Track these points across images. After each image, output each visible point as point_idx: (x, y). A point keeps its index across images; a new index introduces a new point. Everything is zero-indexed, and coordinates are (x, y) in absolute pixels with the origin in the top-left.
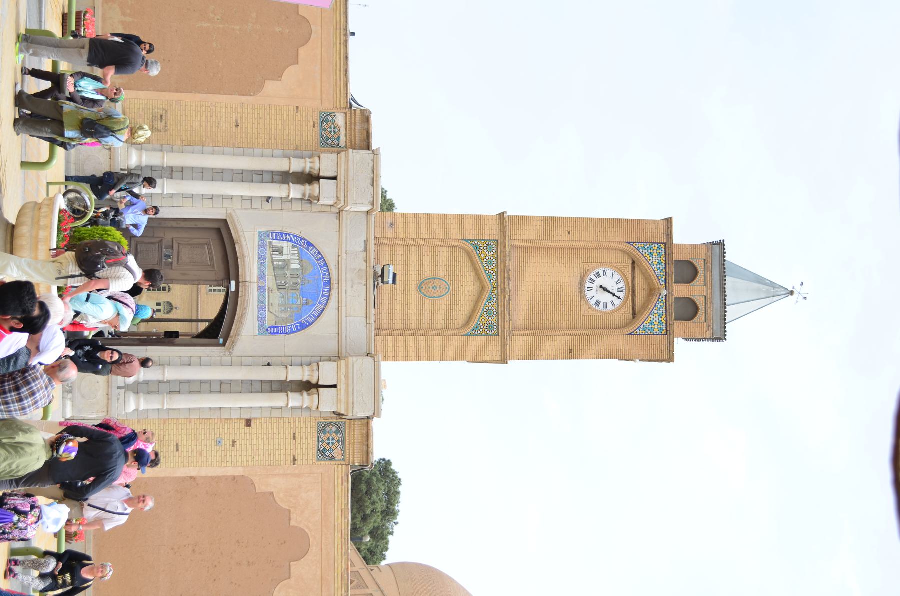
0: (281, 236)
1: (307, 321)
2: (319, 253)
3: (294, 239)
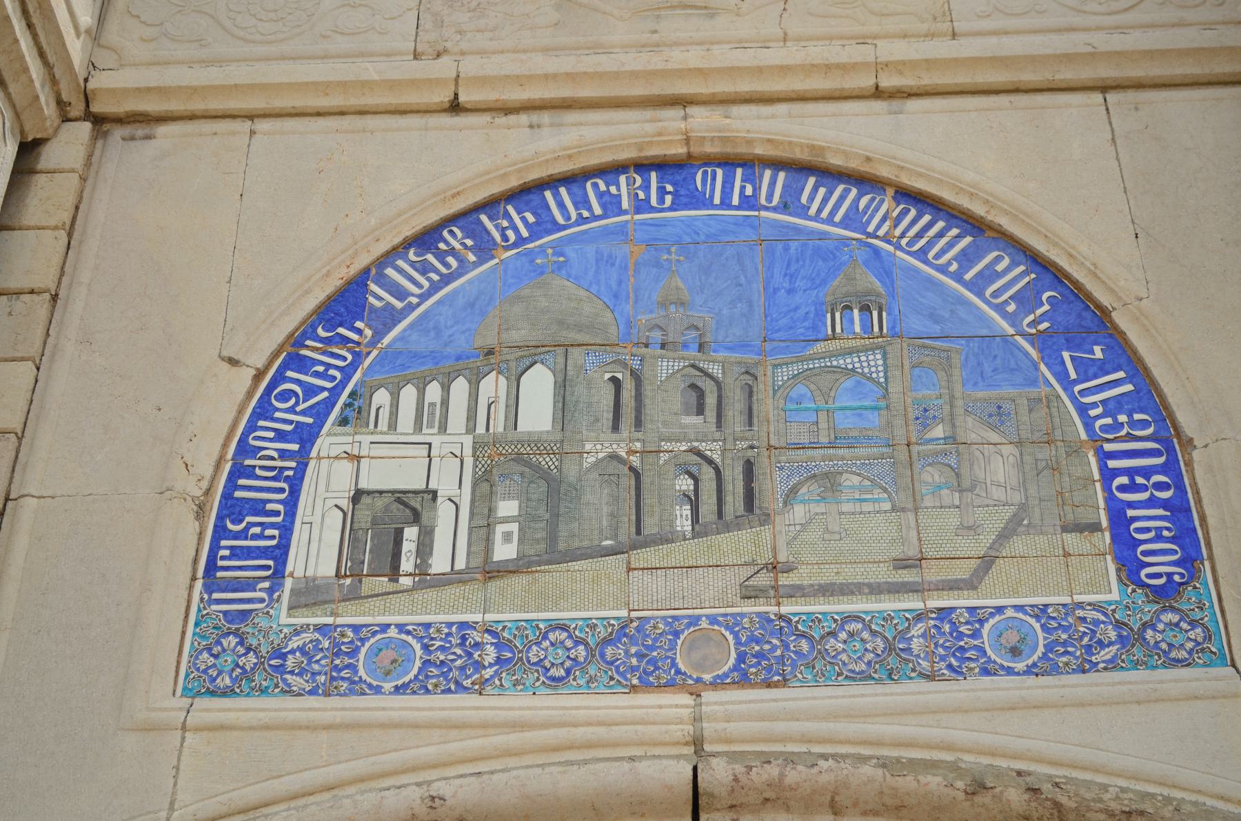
0: (245, 520)
1: (1026, 300)
2: (426, 239)
3: (286, 416)
